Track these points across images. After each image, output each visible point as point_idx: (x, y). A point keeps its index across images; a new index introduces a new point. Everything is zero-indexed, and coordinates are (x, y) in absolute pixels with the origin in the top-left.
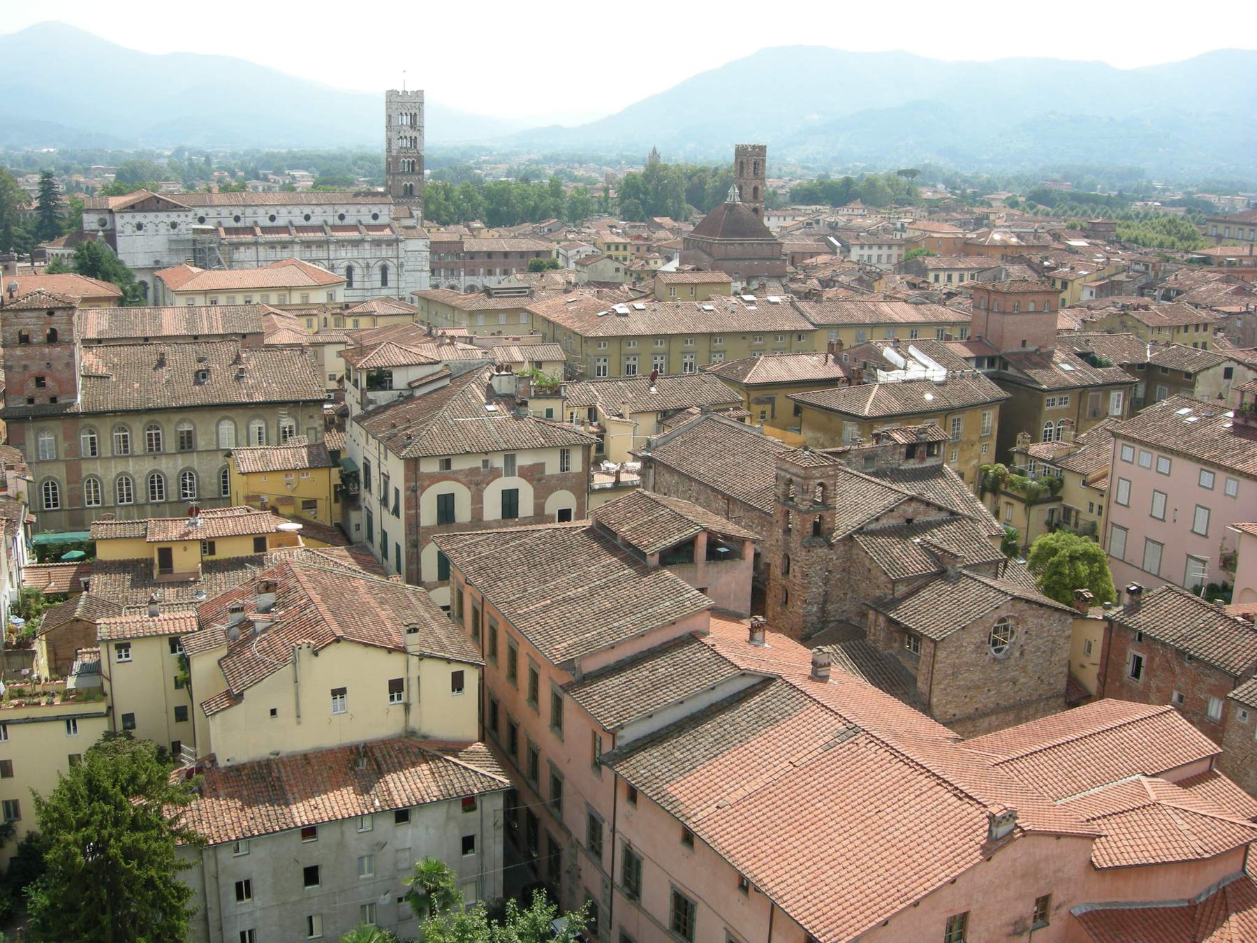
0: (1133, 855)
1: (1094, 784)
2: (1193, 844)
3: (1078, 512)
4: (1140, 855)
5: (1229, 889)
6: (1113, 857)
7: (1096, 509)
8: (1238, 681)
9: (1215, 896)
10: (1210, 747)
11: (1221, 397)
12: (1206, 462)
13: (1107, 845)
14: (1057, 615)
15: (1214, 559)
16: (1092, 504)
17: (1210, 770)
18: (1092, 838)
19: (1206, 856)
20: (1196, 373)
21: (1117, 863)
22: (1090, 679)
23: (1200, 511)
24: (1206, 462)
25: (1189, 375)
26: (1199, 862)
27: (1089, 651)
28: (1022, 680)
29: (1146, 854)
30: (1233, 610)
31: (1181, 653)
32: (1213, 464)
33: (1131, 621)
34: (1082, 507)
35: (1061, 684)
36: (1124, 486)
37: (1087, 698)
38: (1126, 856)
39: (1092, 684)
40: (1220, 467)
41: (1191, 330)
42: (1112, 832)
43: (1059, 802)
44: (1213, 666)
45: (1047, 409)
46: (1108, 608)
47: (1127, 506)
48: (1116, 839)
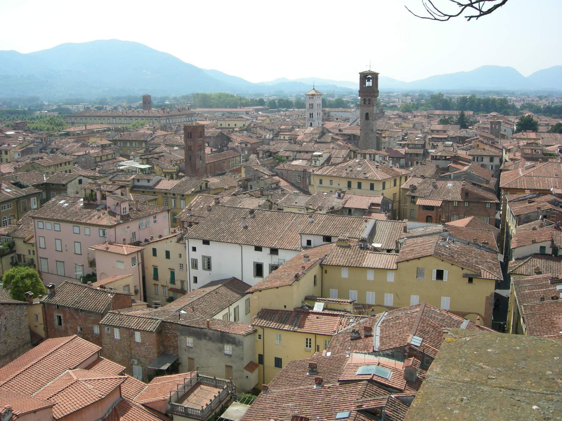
0: (72, 408)
1: (48, 381)
2: (97, 394)
3: (24, 256)
4: (75, 407)
5: (117, 407)
6: (63, 412)
7: (32, 252)
8: (103, 315)
9: (112, 412)
10: (96, 348)
11: (77, 193)
12: (74, 223)
13: (59, 407)
14: (18, 307)
15: (87, 264)
16: (29, 251)
17: (99, 358)
18: (51, 407)
19: (103, 397)
20: (67, 184)
21: (65, 414)
22: (41, 331)
23: (77, 244)
24: (74, 223)
25: (64, 185)
26: (101, 400)
27: (37, 319)
28: (9, 341)
29: (77, 405)
30: (96, 285)
31: (77, 310)
32: (78, 223)
33: (52, 301)
34: (26, 253)
35: (28, 337)
36: (42, 240)
37: (41, 340)
38: (69, 409)
39: (42, 333)
40: (81, 223)
41: (63, 165)
42: (60, 401)
43: (34, 394)
44: (91, 312)
45: (2, 211)
46: (41, 298)
47: (45, 248)
48: (62, 403)
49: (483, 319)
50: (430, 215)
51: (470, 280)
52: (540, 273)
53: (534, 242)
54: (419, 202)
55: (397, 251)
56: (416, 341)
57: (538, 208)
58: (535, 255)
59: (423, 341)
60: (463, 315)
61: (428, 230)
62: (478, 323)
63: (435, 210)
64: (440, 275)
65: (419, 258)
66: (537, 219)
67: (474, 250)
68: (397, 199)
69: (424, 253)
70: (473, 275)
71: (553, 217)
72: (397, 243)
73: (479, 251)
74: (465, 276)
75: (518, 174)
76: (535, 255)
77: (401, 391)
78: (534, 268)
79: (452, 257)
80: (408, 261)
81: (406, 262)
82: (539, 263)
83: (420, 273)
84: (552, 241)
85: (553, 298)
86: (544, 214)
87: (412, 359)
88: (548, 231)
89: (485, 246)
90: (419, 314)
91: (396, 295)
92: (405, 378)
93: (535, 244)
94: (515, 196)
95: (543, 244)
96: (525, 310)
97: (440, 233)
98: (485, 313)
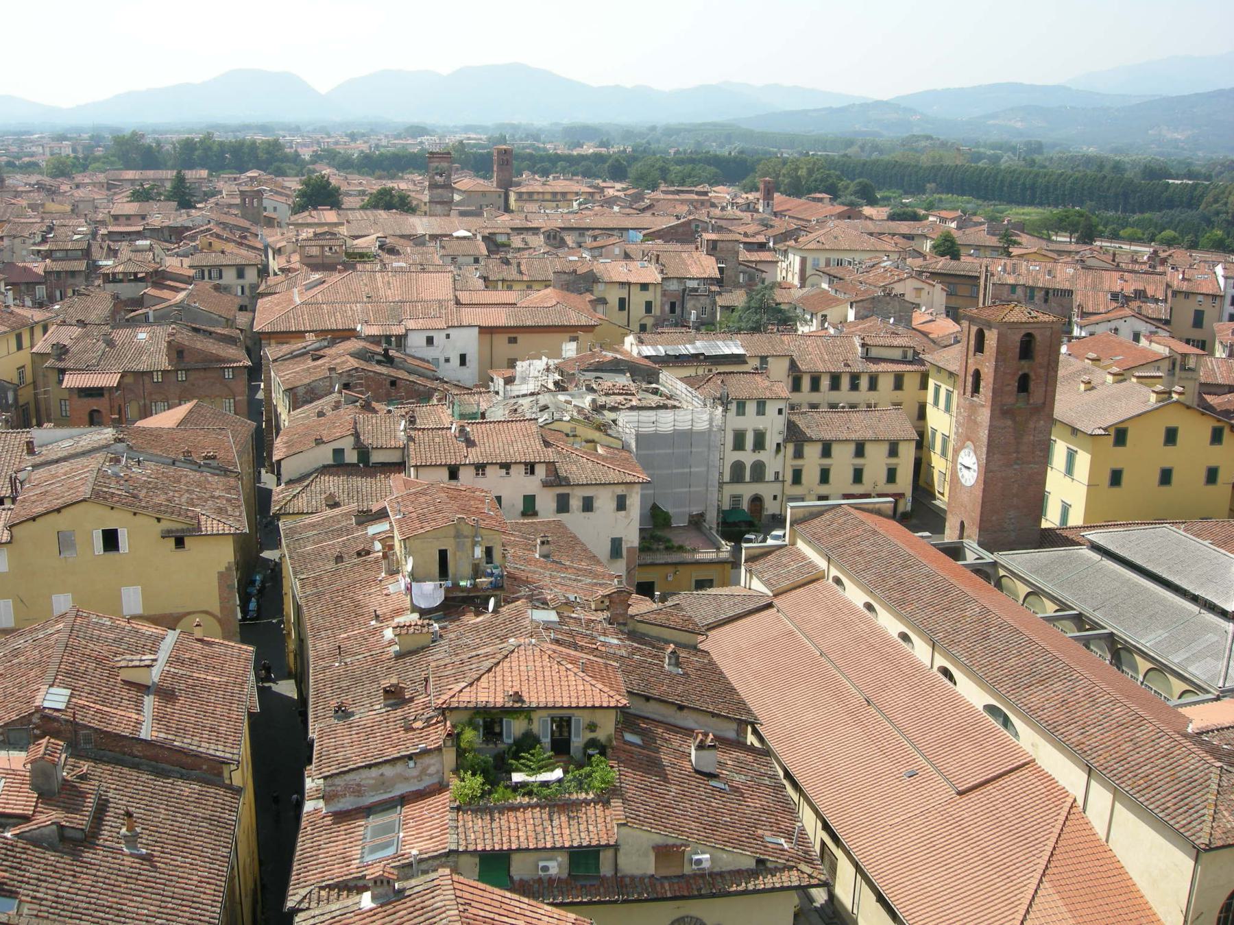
49: (219, 621)
50: (95, 407)
51: (180, 543)
52: (336, 505)
53: (319, 442)
54: (70, 381)
55: (14, 500)
56: (55, 698)
57: (331, 369)
58: (325, 470)
59: (72, 696)
60: (170, 621)
61: (82, 443)
62: (198, 633)
63: (107, 395)
64: (111, 540)
65: (58, 510)
66: (331, 393)
67: (186, 476)
68: (29, 377)
69: (68, 499)
70: (183, 530)
71: (361, 385)
72: (13, 482)
73: (198, 475)
74: (166, 535)
75: (291, 300)
76: (325, 470)
77: (26, 819)
78: (323, 496)
79: (135, 496)
80: (34, 519)
81: (31, 523)
82: (332, 484)
83: (64, 542)
84: (357, 435)
85: (359, 554)
86: (344, 380)
87: (44, 741)
88: (348, 414)
89: (214, 465)
90: (63, 637)
91: (20, 601)
92: (35, 787)
93: (322, 447)
94: (285, 349)
95: (337, 445)
96: (303, 586)
97: (107, 446)
98: (222, 609)
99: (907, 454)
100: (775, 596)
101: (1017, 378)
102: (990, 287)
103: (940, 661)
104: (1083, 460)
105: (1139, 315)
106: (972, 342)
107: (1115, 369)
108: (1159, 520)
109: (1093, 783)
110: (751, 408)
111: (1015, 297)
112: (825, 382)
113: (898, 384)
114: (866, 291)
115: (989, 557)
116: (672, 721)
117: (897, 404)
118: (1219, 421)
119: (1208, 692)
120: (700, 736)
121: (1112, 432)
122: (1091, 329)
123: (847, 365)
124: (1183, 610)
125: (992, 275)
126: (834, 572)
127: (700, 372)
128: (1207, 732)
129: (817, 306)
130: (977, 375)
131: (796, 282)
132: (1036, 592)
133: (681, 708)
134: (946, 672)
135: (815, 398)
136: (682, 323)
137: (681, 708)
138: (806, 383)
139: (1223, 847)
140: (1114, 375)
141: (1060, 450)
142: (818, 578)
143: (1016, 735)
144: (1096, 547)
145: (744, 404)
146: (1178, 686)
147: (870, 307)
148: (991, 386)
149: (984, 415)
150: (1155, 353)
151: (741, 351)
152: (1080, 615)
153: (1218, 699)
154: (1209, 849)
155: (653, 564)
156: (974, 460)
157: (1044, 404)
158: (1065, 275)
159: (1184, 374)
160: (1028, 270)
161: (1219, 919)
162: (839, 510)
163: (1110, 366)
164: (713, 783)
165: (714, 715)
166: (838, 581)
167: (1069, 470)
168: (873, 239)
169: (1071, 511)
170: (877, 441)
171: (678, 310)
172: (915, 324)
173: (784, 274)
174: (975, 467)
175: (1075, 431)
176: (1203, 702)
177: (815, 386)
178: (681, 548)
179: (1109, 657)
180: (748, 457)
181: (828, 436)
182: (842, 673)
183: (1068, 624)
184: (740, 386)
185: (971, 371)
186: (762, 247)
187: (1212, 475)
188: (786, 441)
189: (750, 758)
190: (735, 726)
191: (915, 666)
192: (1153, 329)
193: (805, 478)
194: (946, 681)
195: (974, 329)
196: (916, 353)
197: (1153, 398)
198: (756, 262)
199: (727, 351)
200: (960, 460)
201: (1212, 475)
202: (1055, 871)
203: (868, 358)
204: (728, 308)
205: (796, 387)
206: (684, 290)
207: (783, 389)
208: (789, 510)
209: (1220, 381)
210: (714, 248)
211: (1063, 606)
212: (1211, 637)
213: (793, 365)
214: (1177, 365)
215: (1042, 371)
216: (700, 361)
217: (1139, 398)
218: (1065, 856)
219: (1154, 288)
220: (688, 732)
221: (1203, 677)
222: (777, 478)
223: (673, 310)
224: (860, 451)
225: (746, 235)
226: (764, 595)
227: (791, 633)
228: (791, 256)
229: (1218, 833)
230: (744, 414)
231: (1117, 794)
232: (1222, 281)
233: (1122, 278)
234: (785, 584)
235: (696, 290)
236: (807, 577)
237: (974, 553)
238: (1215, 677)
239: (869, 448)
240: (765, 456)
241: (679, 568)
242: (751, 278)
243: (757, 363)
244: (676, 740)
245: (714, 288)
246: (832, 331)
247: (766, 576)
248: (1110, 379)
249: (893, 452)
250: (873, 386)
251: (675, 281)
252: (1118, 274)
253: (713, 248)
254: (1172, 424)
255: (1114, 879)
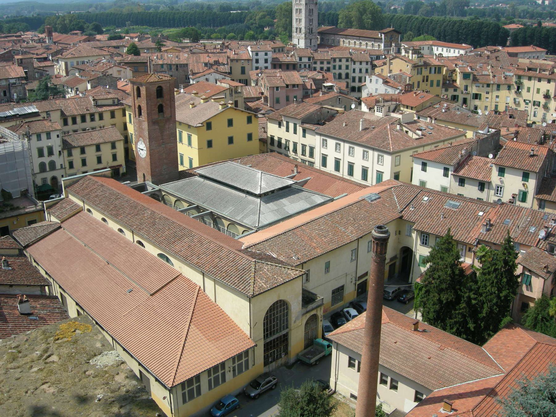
99: (120, 147)
100: (62, 222)
101: (157, 107)
102: (152, 66)
103: (137, 238)
104: (195, 138)
105: (217, 72)
106: (135, 93)
107: (204, 97)
108: (232, 159)
109: (206, 279)
110: (44, 136)
111: (163, 69)
112: (79, 120)
113: (113, 116)
114: (95, 75)
115: (157, 188)
116: (8, 292)
117: (114, 125)
118: (249, 113)
119: (253, 230)
120: (20, 298)
121: (205, 125)
122: (197, 80)
123: (87, 110)
124: (239, 196)
125: (152, 61)
126: (87, 207)
127: (18, 123)
128: (250, 247)
129: (74, 84)
130: (140, 107)
131: (64, 74)
132: (179, 200)
133: (11, 286)
134: (140, 243)
135: (75, 127)
136: (10, 100)
137: (11, 286)
138: (70, 121)
139: (259, 294)
140: (203, 99)
141: (185, 135)
142: (81, 210)
143: (173, 265)
144: (202, 176)
145: (40, 135)
146: (241, 229)
147: (97, 82)
148: (146, 112)
149: (145, 125)
150: (223, 87)
151: (36, 110)
152: (198, 207)
153: (257, 231)
154: (254, 296)
155: (5, 218)
156: (144, 146)
157: (171, 116)
158: (184, 57)
159: (237, 95)
160: (168, 57)
161: (264, 323)
162: (85, 178)
163: (202, 96)
164: (31, 318)
165: (28, 286)
166: (89, 211)
167: (190, 144)
168: (97, 50)
169: (193, 161)
170: (105, 143)
171: (8, 94)
172: (119, 87)
173: (58, 71)
174: (145, 149)
175: (189, 126)
176: (251, 234)
177: (74, 122)
178: (18, 208)
179: (212, 222)
180: (46, 160)
181: (82, 144)
182: (95, 252)
183: (194, 211)
184: (38, 126)
185: (137, 106)
186: (46, 59)
187: (250, 137)
188: (63, 149)
189: (48, 302)
190: (39, 288)
191: (127, 242)
192: (223, 77)
193: (75, 165)
194: (141, 246)
195: (135, 87)
196: (119, 100)
197: (220, 107)
198: (43, 67)
199: (30, 111)
200: (138, 147)
201: (250, 137)
202: (195, 319)
203: (97, 106)
204: (31, 90)
205: (66, 123)
206: (9, 85)
207: (58, 125)
208: (62, 182)
209: (253, 96)
210: (22, 63)
211: (191, 204)
212: (252, 206)
213: (62, 114)
214: (233, 91)
215: (168, 102)
216: (17, 118)
217: (215, 108)
218: (199, 312)
219: (222, 59)
220: (14, 296)
221: (250, 224)
222: (62, 167)
223: (5, 94)
224: (98, 148)
225: (37, 54)
226: (57, 223)
227: (71, 238)
228: (60, 62)
229: (256, 289)
230: (41, 140)
231: (214, 281)
232: (250, 53)
233: (208, 56)
234: (65, 216)
235: (15, 84)
236: (76, 211)
237: (151, 187)
238: (254, 223)
239: (102, 147)
240: (55, 158)
241: (19, 217)
242: (42, 75)
243: (44, 115)
244: (10, 301)
245: (23, 82)
246: (81, 95)
247: (57, 214)
248: (202, 101)
249: (114, 147)
250: (101, 118)
251: (4, 81)
252: (206, 55)
253: (21, 63)
254: (230, 118)
255: (220, 317)
